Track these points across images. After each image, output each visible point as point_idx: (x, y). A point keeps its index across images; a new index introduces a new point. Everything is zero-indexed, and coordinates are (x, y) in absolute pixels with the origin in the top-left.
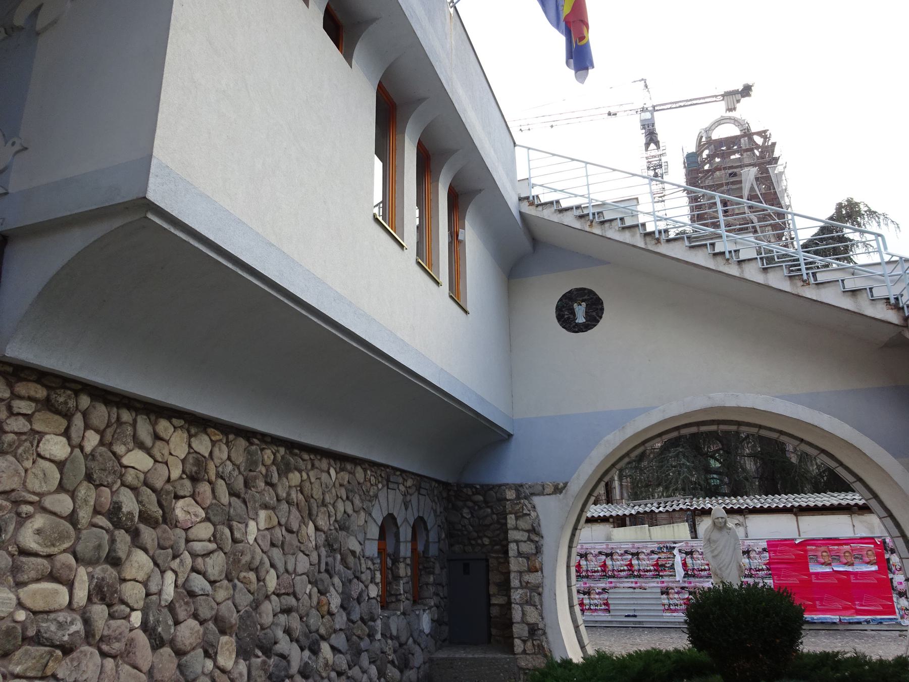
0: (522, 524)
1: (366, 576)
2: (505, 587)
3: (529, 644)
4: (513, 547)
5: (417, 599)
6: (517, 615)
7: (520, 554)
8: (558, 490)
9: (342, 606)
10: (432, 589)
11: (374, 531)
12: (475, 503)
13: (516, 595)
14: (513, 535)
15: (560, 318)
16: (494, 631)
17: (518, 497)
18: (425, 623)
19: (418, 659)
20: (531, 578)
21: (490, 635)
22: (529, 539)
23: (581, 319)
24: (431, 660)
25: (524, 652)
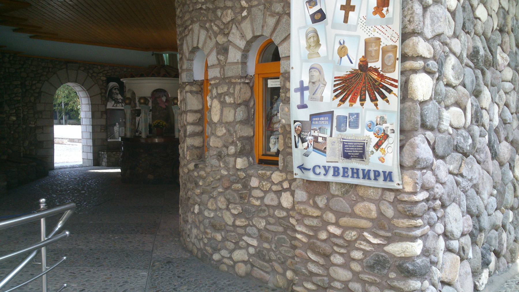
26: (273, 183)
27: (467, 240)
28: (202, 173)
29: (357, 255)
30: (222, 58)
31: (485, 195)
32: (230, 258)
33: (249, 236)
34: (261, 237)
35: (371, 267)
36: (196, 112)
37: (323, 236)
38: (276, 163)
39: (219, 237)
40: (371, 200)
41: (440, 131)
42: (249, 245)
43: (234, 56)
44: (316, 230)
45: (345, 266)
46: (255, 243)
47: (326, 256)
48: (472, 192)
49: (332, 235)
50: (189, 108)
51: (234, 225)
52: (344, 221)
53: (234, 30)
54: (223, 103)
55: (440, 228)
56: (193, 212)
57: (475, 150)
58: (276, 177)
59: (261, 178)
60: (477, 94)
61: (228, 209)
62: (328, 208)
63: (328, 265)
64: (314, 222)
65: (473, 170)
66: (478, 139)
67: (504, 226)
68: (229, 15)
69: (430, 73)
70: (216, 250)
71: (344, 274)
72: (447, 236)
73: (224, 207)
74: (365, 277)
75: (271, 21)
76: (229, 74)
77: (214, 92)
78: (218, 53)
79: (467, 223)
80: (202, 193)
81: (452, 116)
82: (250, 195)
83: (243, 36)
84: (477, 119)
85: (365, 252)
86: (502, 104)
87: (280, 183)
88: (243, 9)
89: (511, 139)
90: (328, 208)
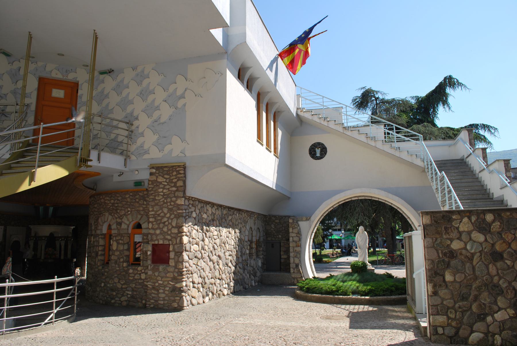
0: (295, 231)
1: (246, 247)
2: (287, 252)
3: (296, 270)
4: (291, 239)
5: (257, 256)
6: (292, 260)
7: (293, 241)
8: (308, 219)
9: (241, 256)
10: (261, 252)
11: (247, 233)
12: (276, 223)
13: (292, 255)
14: (291, 235)
15: (310, 153)
16: (282, 267)
17: (293, 222)
18: (260, 264)
19: (258, 274)
20: (297, 249)
21: (281, 268)
22: (297, 236)
23: (318, 155)
24: (262, 275)
25: (294, 272)
26: (138, 271)
27: (200, 285)
28: (107, 270)
29: (167, 289)
30: (119, 227)
31: (207, 273)
32: (120, 300)
33: (128, 291)
34: (133, 290)
35: (171, 292)
36: (102, 246)
37: (157, 284)
38: (140, 264)
39: (114, 293)
40: (171, 272)
41: (190, 252)
42: (128, 294)
43: (124, 226)
44: (155, 283)
45: (164, 293)
46: (130, 293)
47: (158, 291)
48: (202, 271)
49: (159, 284)
50: (100, 244)
51: (122, 288)
52: (164, 279)
53: (125, 217)
54: (118, 243)
55: (191, 280)
56: (101, 286)
57: (202, 258)
58: (140, 268)
59: (134, 270)
60: (203, 240)
61: (119, 282)
62: (159, 276)
63: (159, 293)
64: (154, 281)
65: (201, 263)
66: (203, 254)
67: (215, 284)
68: (123, 212)
69: (187, 236)
70: (112, 299)
71: (163, 295)
72: (193, 283)
73: (117, 281)
74: (170, 295)
75: (139, 216)
76: (122, 232)
77: (114, 239)
78: (117, 224)
79: (200, 280)
80: (106, 278)
81: (195, 247)
82: (129, 276)
83: (128, 220)
84: (203, 248)
85: (170, 288)
86: (213, 243)
87: (141, 271)
88: (129, 211)
89: (217, 255)
90: (159, 276)
